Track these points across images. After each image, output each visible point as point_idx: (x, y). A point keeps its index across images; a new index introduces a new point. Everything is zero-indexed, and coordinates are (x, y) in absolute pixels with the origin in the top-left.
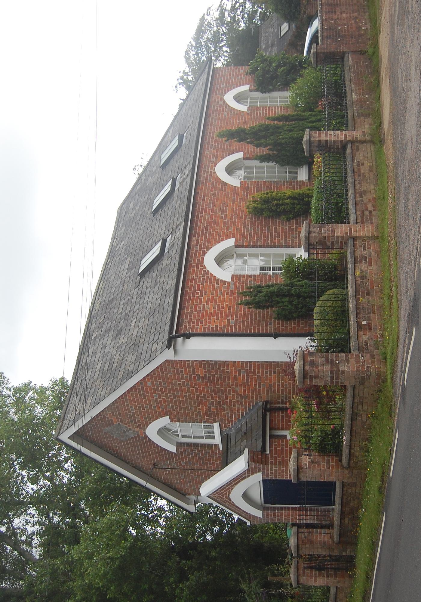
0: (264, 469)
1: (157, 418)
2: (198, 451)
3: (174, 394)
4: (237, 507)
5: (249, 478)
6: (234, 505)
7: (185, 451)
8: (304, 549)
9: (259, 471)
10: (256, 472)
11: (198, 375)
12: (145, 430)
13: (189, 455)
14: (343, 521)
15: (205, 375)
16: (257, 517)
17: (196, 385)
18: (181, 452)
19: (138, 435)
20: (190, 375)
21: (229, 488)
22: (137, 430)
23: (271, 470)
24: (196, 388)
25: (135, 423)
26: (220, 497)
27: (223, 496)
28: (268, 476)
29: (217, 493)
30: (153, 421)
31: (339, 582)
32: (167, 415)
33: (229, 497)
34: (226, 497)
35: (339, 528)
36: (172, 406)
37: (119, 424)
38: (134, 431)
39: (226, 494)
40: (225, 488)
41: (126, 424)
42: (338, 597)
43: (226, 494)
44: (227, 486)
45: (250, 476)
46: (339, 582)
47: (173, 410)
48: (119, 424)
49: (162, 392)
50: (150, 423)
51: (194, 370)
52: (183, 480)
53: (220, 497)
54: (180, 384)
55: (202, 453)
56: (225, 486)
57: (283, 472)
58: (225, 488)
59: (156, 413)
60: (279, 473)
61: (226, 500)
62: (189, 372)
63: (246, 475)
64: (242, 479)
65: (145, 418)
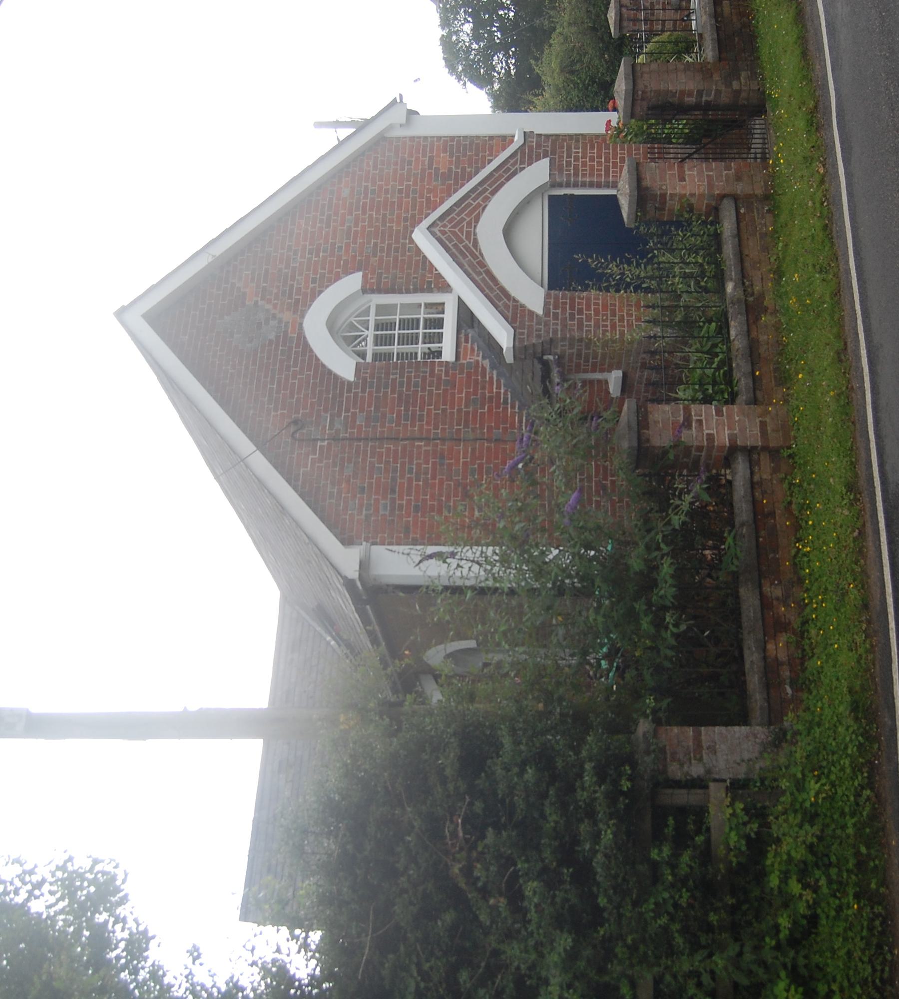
0: (553, 152)
1: (338, 278)
2: (402, 376)
3: (384, 215)
4: (489, 273)
5: (523, 172)
6: (482, 264)
7: (372, 376)
8: (646, 76)
9: (545, 156)
10: (538, 159)
11: (437, 169)
12: (303, 316)
13: (378, 391)
14: (719, 10)
15: (450, 170)
16: (531, 313)
17: (429, 191)
18: (365, 379)
19: (286, 333)
20: (423, 170)
21: (479, 205)
22: (287, 316)
23: (569, 156)
24: (428, 199)
25: (290, 297)
26: (454, 233)
27: (461, 230)
28: (561, 170)
29: (450, 221)
30: (327, 287)
31: (738, 178)
32: (359, 270)
33: (475, 234)
34: (468, 233)
35: (713, 21)
36: (376, 244)
37: (256, 303)
38: (280, 321)
39: (469, 224)
40: (470, 204)
41: (269, 301)
42: (746, 252)
43: (469, 224)
44: (474, 199)
45: (524, 168)
46: (738, 178)
47: (375, 255)
48: (256, 302)
49: (364, 213)
50: (320, 292)
51: (431, 158)
52: (348, 481)
53: (454, 233)
54: (400, 191)
55: (409, 378)
56: (469, 200)
57: (592, 159)
58: (470, 204)
59: (338, 266)
60: (584, 164)
61: (466, 247)
62: (423, 162)
63: (517, 166)
64: (508, 179)
65: (314, 281)
